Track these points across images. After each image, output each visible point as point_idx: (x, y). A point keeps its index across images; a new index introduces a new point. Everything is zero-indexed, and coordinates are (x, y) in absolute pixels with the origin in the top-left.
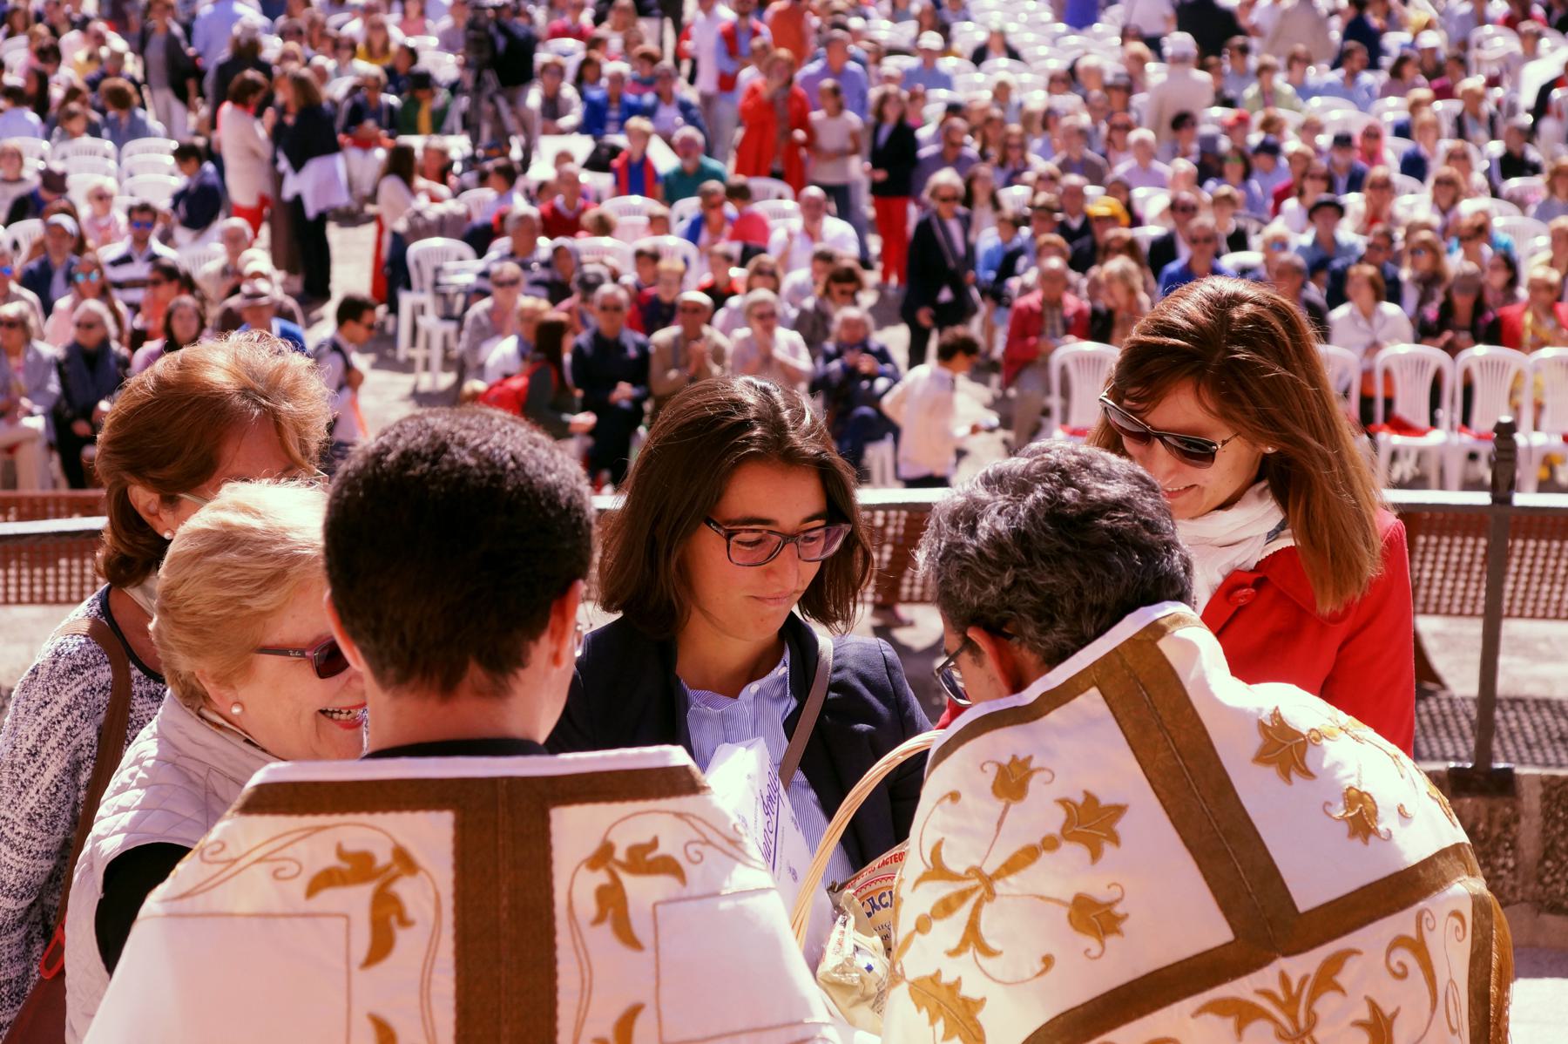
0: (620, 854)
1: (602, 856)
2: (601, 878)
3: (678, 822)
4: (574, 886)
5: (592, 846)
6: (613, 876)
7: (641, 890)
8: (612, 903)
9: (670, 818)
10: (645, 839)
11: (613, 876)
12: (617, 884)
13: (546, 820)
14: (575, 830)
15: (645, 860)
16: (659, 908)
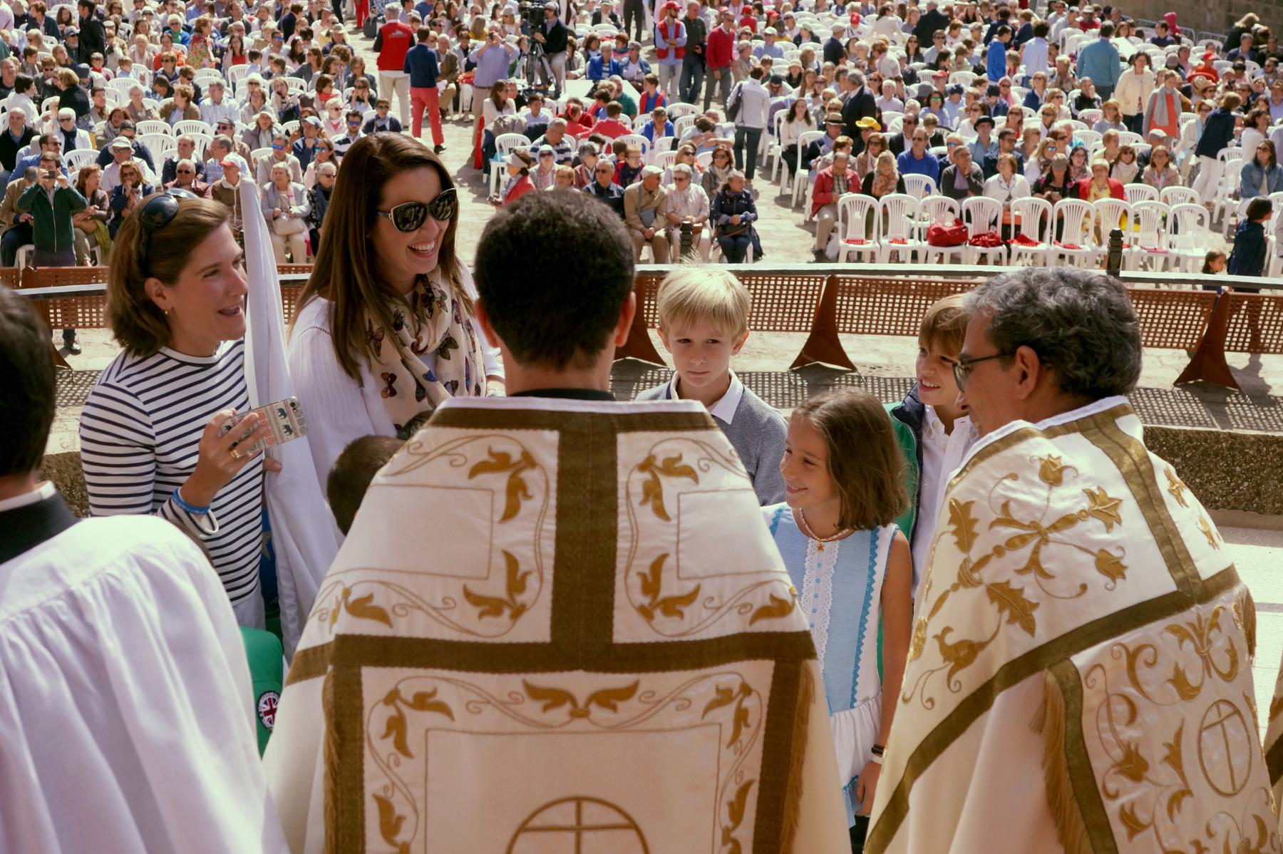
0: (659, 463)
1: (647, 465)
2: (647, 476)
3: (696, 446)
4: (630, 480)
5: (641, 458)
6: (654, 476)
7: (671, 486)
8: (653, 493)
9: (690, 443)
10: (675, 455)
11: (654, 476)
12: (657, 483)
13: (613, 444)
14: (631, 447)
15: (674, 468)
16: (682, 497)
